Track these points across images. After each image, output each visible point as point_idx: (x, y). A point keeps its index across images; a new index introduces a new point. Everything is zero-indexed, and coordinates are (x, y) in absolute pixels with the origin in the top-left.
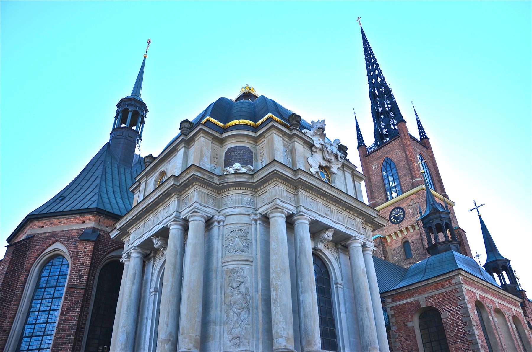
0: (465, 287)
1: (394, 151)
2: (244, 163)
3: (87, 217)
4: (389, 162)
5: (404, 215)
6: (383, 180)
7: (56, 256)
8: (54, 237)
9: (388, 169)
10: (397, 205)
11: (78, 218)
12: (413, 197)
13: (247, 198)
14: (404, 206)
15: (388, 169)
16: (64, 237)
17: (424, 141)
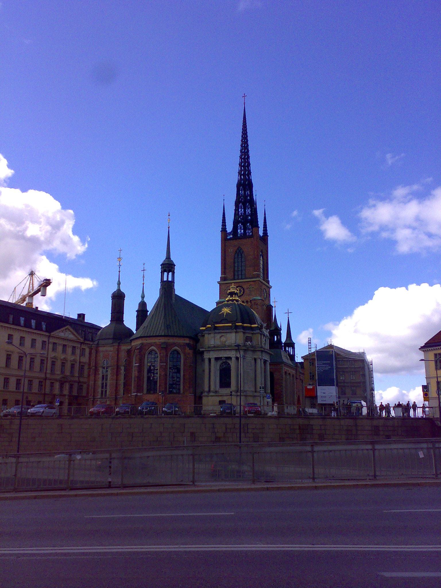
0: (284, 367)
1: (247, 246)
2: (251, 342)
3: (186, 339)
4: (241, 251)
5: (244, 292)
6: (234, 263)
7: (176, 350)
8: (174, 344)
9: (240, 256)
10: (240, 284)
11: (182, 339)
12: (251, 283)
13: (252, 353)
14: (245, 287)
15: (240, 256)
16: (179, 345)
17: (265, 238)
